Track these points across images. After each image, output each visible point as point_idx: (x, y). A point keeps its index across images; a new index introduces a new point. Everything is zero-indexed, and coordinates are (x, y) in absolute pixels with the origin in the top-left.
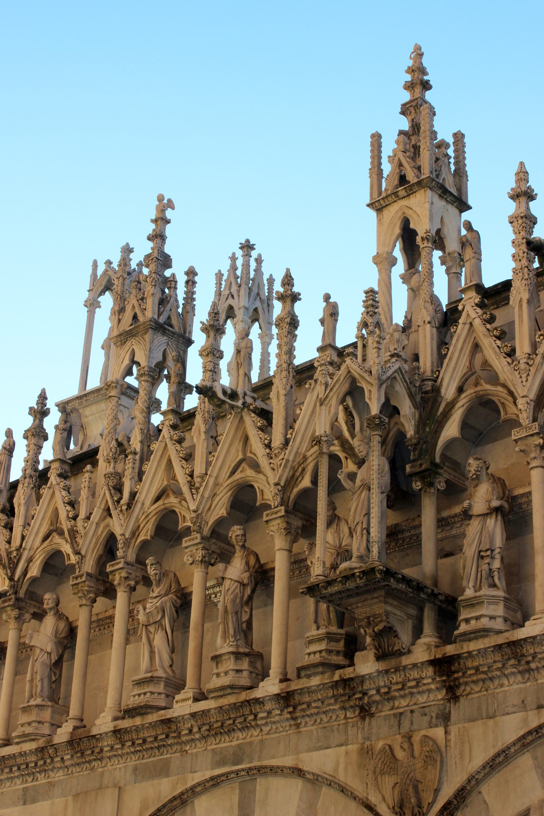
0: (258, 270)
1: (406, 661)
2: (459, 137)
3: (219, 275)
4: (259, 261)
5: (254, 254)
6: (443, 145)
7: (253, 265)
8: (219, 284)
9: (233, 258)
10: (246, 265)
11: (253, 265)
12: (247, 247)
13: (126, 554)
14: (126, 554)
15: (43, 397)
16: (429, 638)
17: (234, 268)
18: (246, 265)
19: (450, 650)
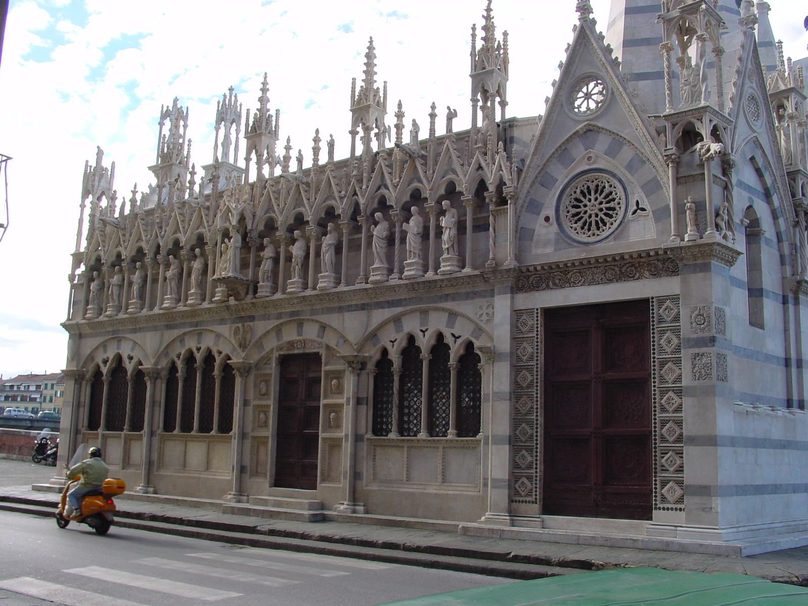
0: (236, 100)
1: (243, 302)
2: (278, 111)
3: (219, 102)
4: (236, 96)
5: (234, 92)
6: (270, 116)
7: (233, 98)
8: (218, 107)
9: (225, 96)
10: (230, 100)
11: (233, 98)
12: (231, 90)
13: (163, 252)
14: (163, 252)
15: (135, 187)
16: (250, 296)
17: (224, 100)
18: (230, 100)
19: (254, 301)
